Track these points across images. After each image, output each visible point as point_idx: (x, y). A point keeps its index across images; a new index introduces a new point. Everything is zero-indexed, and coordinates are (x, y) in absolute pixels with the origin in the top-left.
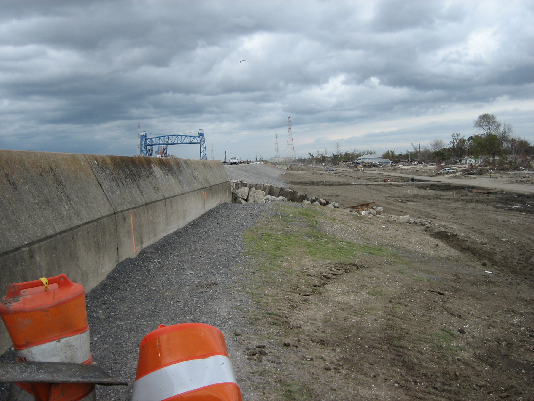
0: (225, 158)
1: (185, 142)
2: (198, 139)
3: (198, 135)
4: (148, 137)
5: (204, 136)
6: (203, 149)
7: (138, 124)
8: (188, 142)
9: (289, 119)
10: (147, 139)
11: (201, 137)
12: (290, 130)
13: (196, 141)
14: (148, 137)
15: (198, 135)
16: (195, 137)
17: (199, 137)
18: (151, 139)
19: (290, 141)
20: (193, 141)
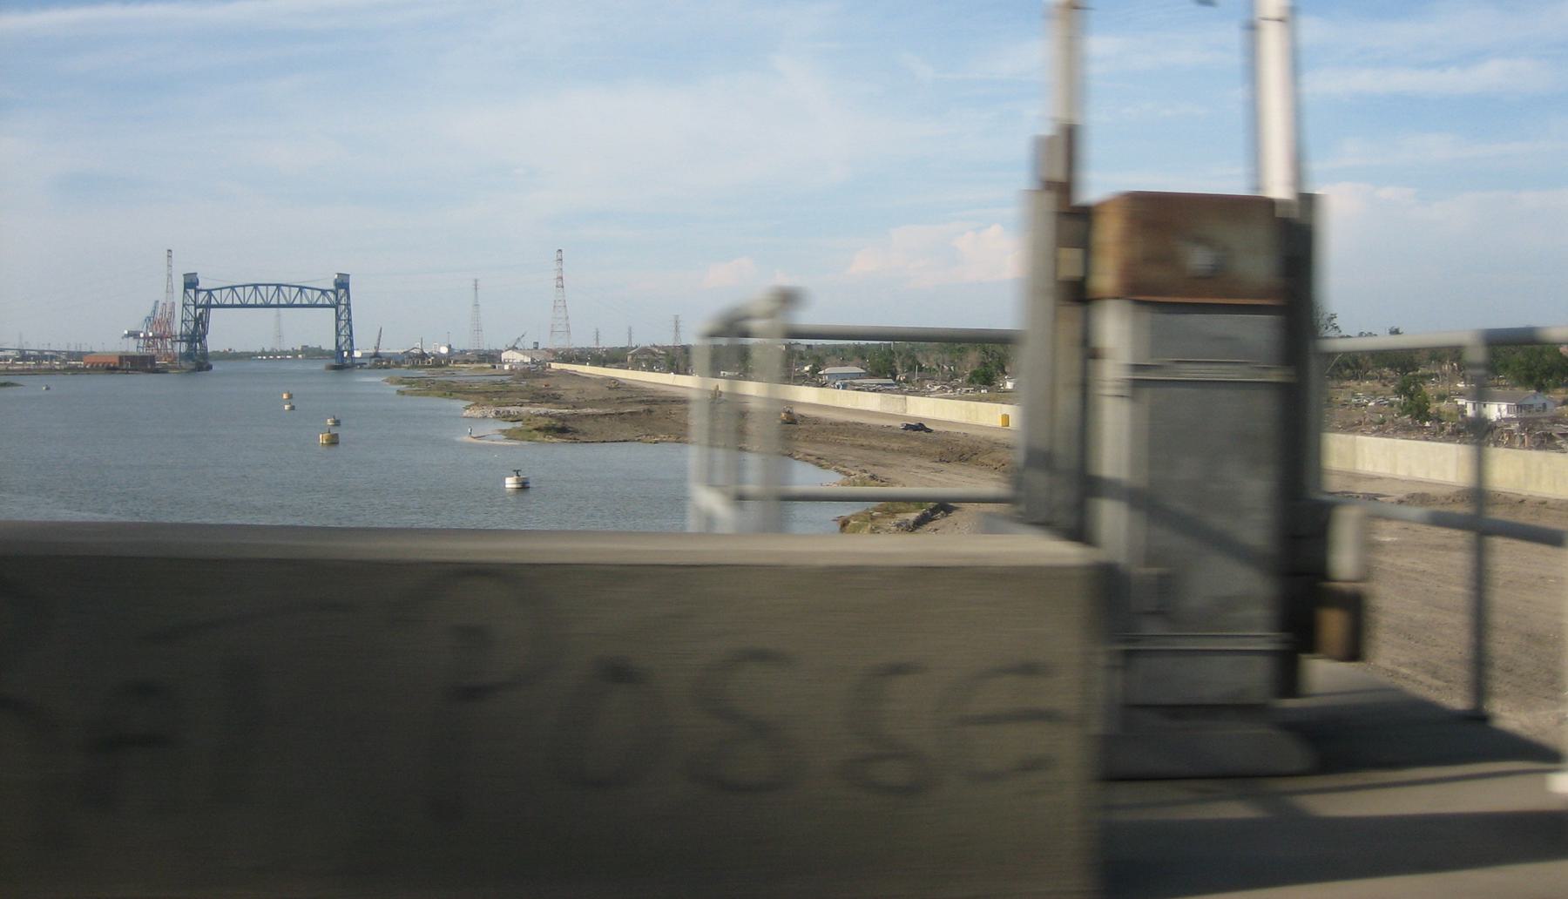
0: (379, 344)
1: (297, 302)
2: (332, 296)
3: (333, 287)
4: (199, 287)
5: (347, 290)
6: (344, 324)
7: (170, 251)
8: (305, 302)
9: (559, 255)
10: (197, 291)
11: (342, 291)
12: (560, 283)
13: (327, 302)
14: (199, 287)
15: (333, 287)
16: (324, 292)
17: (336, 293)
18: (209, 292)
19: (560, 309)
20: (320, 302)
